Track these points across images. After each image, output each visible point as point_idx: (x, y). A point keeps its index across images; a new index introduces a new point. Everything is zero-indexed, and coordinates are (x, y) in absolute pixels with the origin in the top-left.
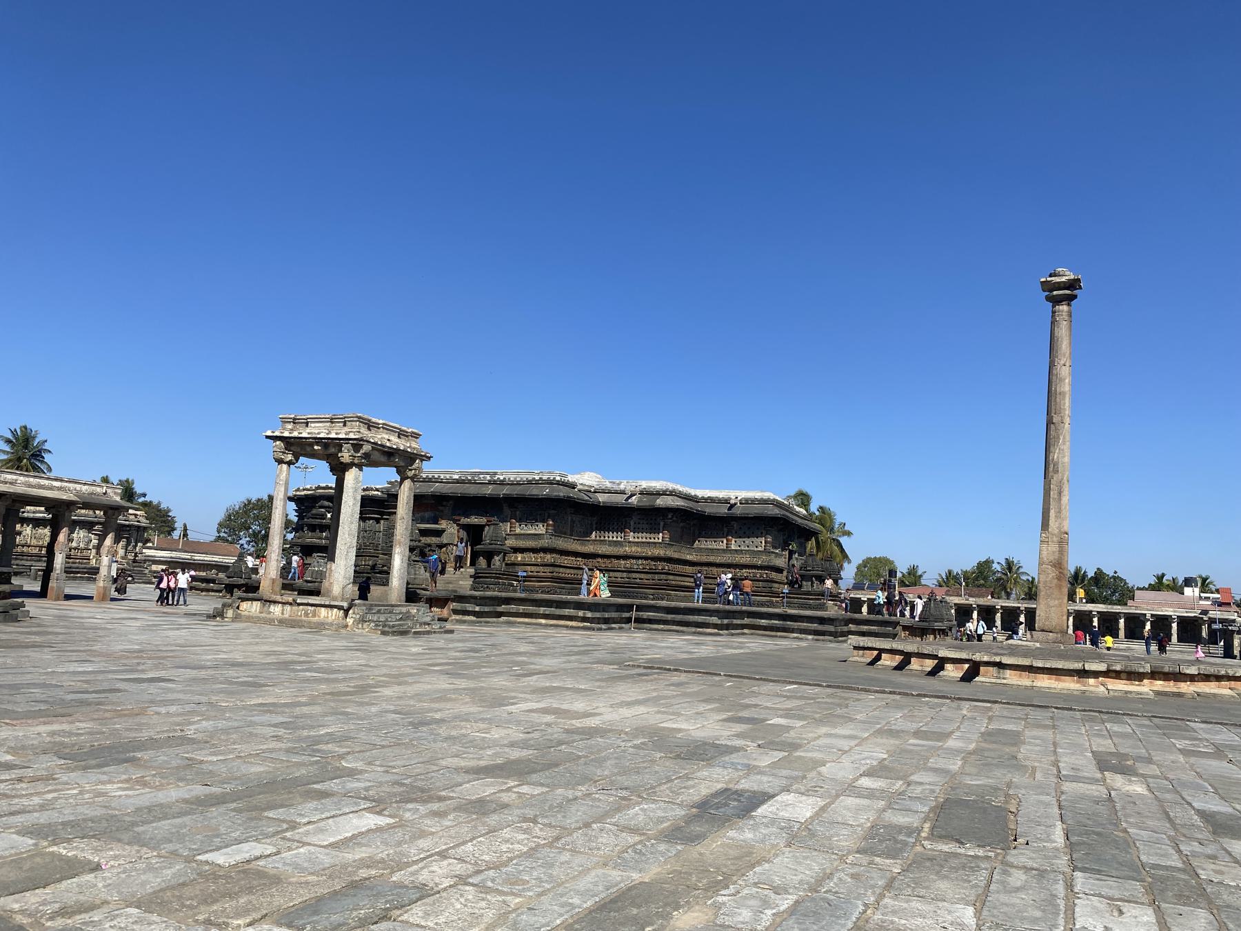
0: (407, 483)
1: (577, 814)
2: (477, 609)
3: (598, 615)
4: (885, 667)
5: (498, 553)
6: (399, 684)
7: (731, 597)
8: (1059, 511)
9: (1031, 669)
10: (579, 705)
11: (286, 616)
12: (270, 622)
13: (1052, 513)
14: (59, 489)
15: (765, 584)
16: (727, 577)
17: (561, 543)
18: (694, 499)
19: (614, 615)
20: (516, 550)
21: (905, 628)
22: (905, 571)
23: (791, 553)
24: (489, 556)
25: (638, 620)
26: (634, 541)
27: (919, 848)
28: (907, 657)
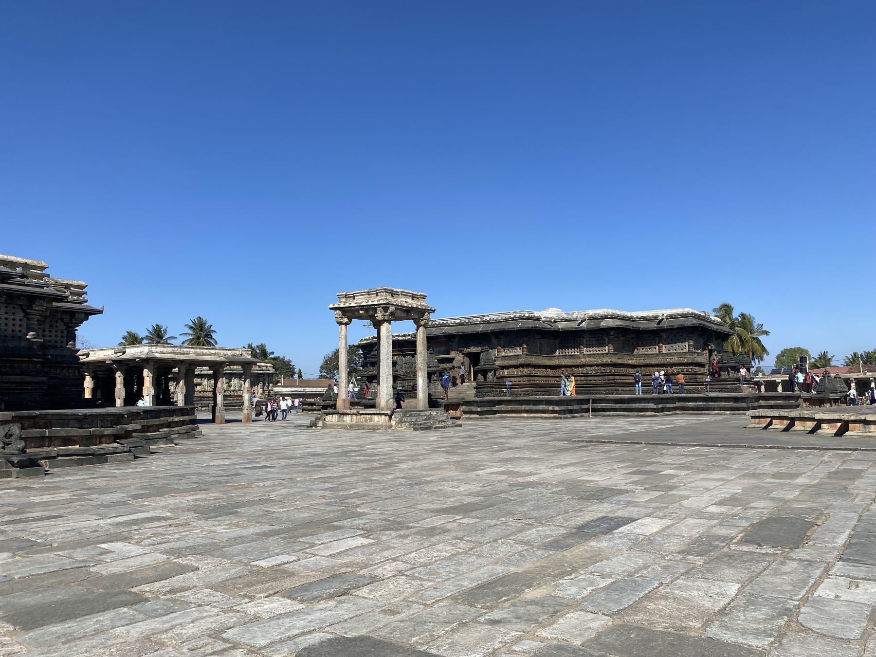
1: (492, 534)
2: (479, 409)
3: (563, 408)
4: (776, 430)
5: (490, 371)
6: (413, 461)
7: (665, 388)
10: (527, 469)
11: (354, 422)
12: (344, 427)
14: (215, 354)
16: (661, 374)
17: (534, 360)
18: (631, 319)
19: (576, 407)
21: (805, 400)
22: (817, 357)
23: (711, 352)
24: (485, 373)
25: (594, 410)
26: (587, 354)
27: (726, 550)
28: (792, 421)
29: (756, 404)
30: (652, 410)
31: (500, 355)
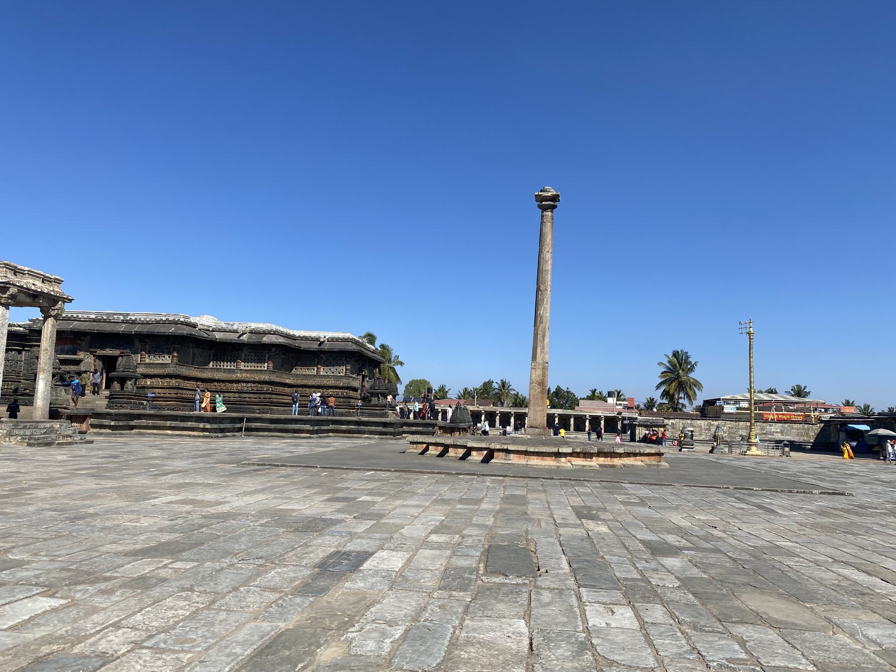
0: (50, 321)
1: (225, 582)
2: (113, 423)
3: (215, 426)
5: (130, 379)
6: (51, 486)
7: (320, 410)
8: (543, 348)
9: (526, 453)
10: (210, 496)
13: (539, 350)
15: (345, 400)
16: (317, 396)
17: (184, 371)
19: (228, 426)
20: (146, 376)
21: (440, 428)
22: (437, 389)
23: (364, 377)
24: (122, 381)
25: (247, 429)
26: (244, 369)
27: (480, 582)
28: (446, 448)
29: (401, 430)
30: (308, 432)
31: (144, 362)
